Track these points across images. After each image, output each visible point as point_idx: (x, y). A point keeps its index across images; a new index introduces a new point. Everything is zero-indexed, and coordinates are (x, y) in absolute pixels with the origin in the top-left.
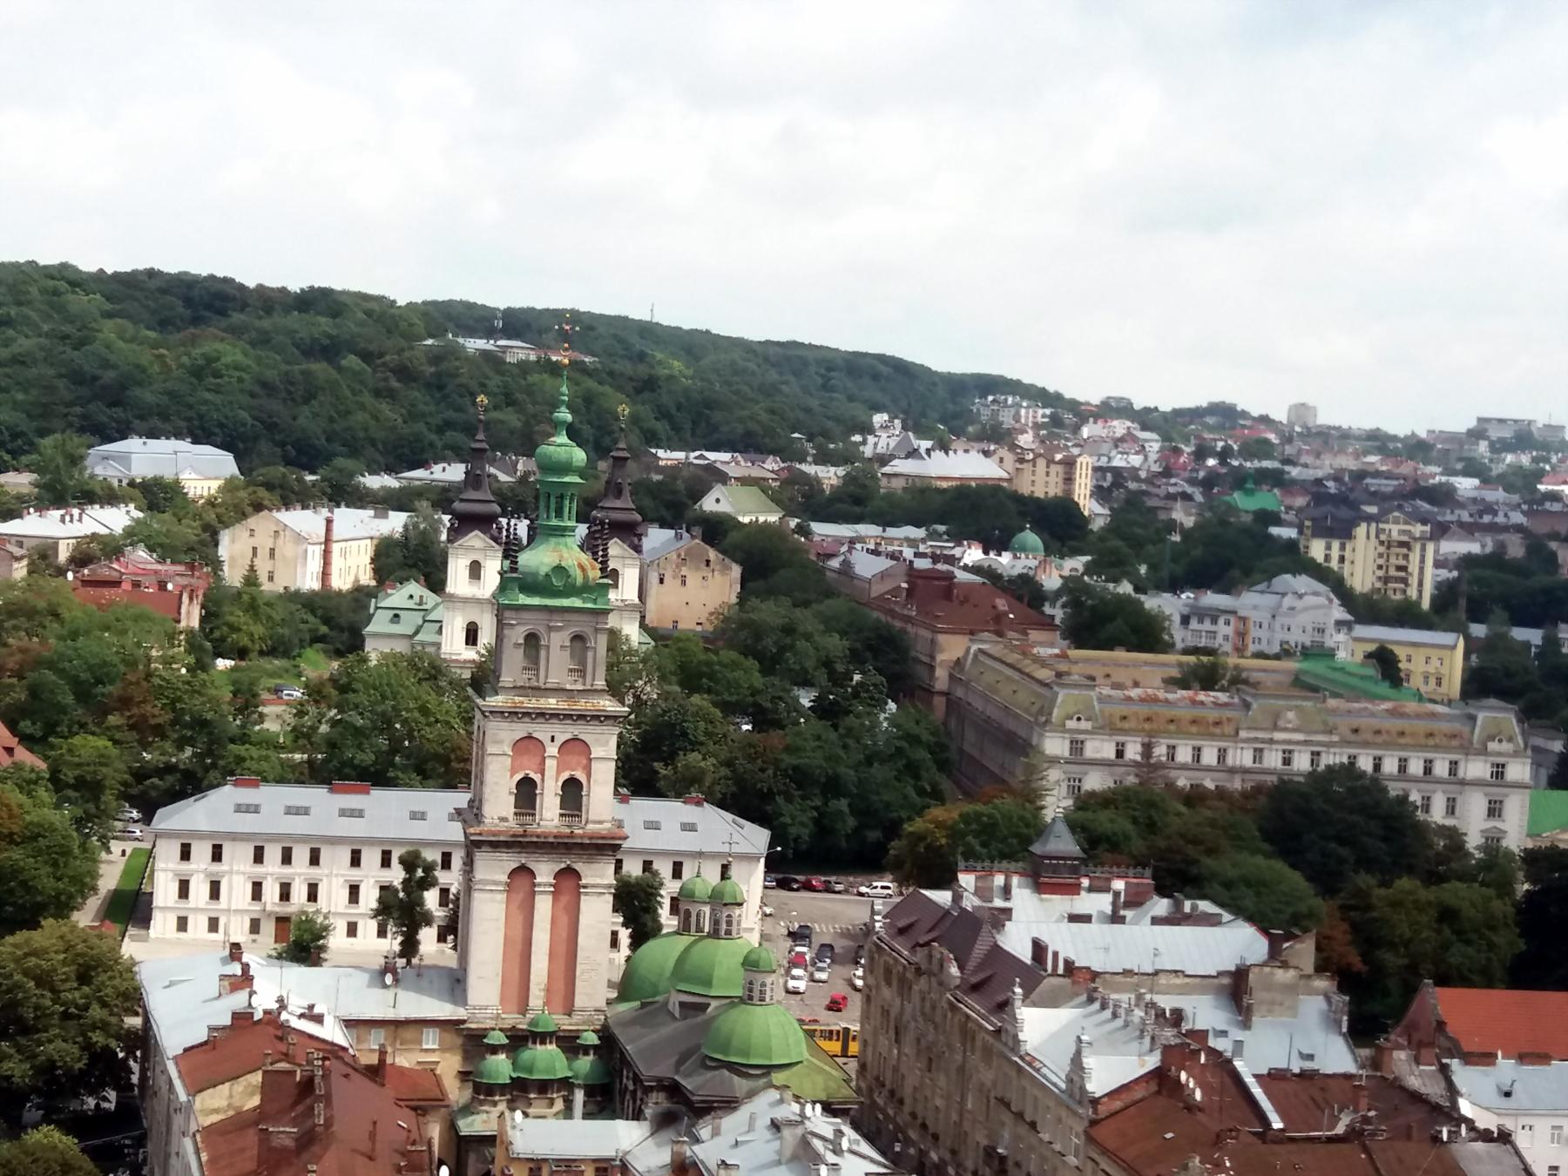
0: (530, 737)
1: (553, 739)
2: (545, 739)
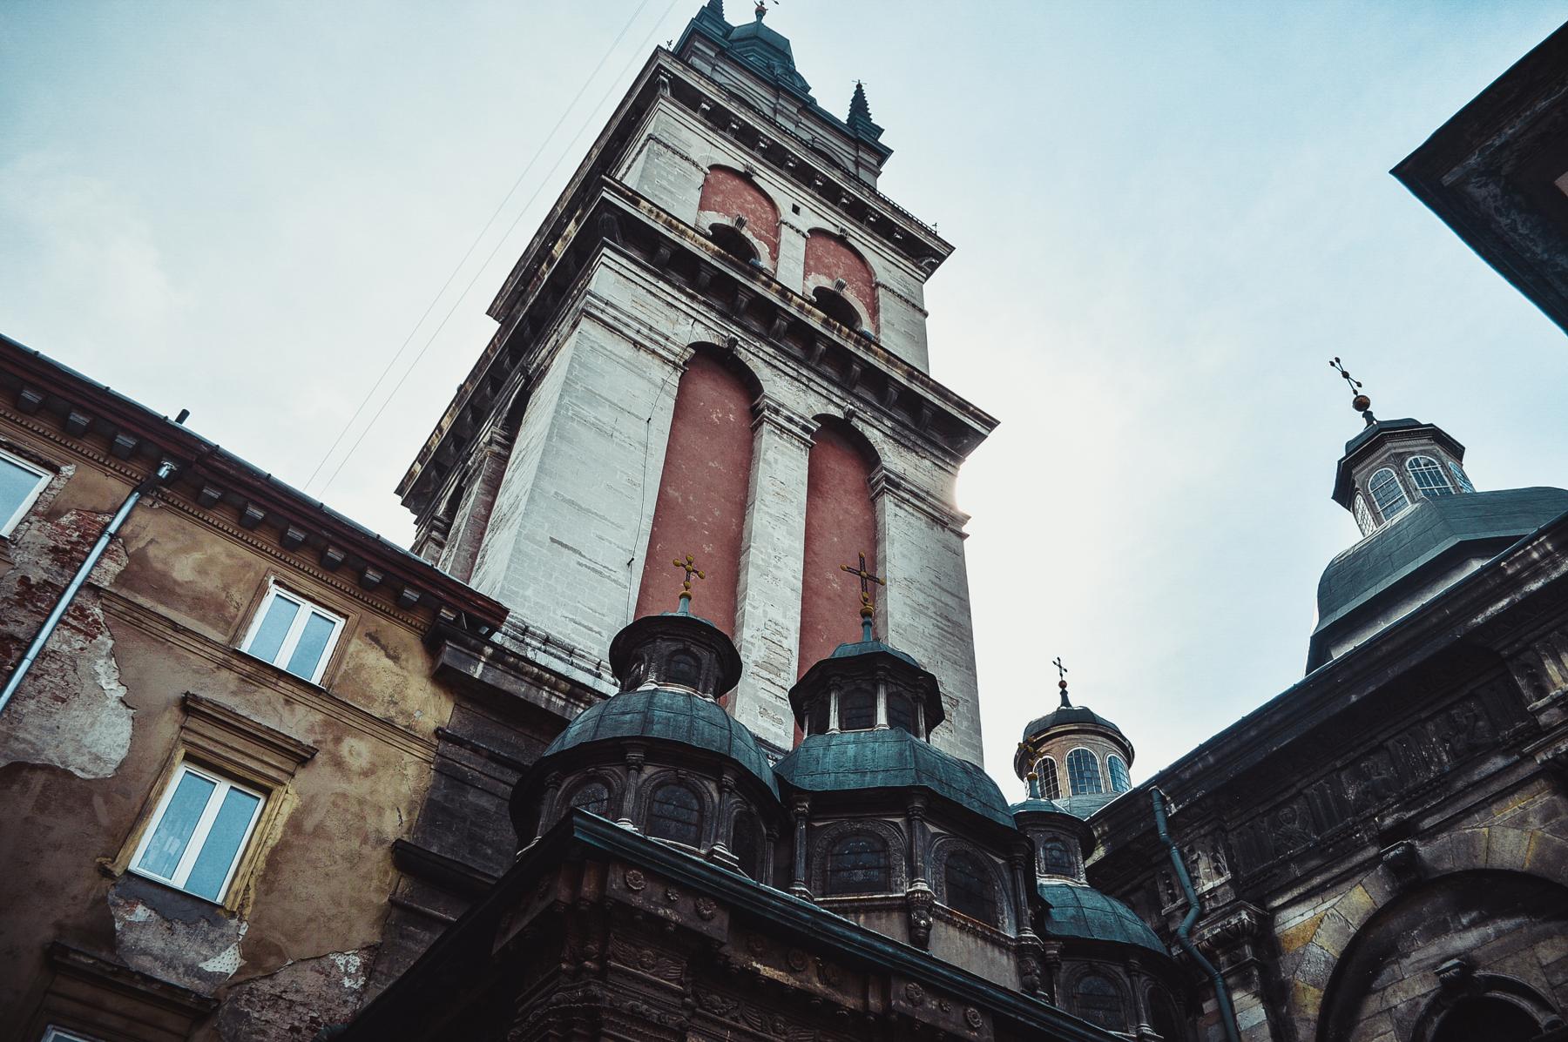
0: (746, 177)
1: (796, 210)
2: (784, 202)
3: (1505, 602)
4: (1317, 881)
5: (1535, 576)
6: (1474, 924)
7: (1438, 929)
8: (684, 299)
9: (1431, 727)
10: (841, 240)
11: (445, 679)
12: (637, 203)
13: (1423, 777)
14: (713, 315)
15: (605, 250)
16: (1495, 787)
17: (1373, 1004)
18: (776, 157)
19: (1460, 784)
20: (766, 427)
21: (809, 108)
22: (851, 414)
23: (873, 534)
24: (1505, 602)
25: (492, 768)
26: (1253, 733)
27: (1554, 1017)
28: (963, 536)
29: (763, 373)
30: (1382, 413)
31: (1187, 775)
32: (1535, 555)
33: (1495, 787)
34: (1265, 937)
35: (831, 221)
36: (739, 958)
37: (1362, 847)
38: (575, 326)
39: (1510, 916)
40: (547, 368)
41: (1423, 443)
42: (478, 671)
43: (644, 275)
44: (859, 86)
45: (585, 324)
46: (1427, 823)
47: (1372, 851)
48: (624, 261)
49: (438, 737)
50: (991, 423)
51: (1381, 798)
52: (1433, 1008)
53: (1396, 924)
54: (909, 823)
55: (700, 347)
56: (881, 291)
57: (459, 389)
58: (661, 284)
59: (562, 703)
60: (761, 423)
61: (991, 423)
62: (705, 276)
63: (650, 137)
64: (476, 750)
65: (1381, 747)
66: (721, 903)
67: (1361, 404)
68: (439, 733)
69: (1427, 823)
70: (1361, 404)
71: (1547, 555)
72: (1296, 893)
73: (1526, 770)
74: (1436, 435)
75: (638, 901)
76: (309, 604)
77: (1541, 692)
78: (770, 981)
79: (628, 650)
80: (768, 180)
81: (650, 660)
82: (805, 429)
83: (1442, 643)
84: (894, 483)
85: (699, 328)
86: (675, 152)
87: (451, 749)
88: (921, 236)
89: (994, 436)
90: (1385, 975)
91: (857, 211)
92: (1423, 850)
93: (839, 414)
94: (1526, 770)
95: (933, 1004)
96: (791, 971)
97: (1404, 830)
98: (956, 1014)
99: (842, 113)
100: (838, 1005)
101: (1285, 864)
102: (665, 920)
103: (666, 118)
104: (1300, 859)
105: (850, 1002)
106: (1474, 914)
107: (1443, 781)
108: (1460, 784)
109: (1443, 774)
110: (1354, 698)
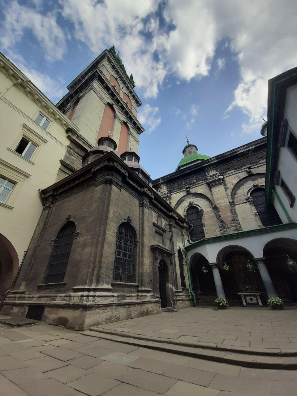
1: (123, 88)
3: (207, 164)
4: (178, 192)
5: (212, 162)
6: (194, 198)
7: (190, 198)
8: (107, 94)
9: (194, 177)
10: (128, 96)
11: (69, 137)
12: (102, 74)
13: (192, 182)
14: (111, 99)
15: (96, 80)
16: (201, 184)
17: (181, 205)
18: (121, 78)
19: (196, 183)
20: (116, 119)
21: (125, 73)
22: (127, 122)
23: (128, 139)
24: (207, 164)
25: (76, 154)
26: (174, 174)
27: (200, 208)
28: (138, 144)
29: (116, 111)
30: (190, 143)
31: (165, 178)
32: (213, 159)
33: (201, 184)
34: (170, 198)
35: (128, 93)
36: (128, 180)
37: (184, 189)
38: (90, 91)
39: (199, 198)
40: (83, 97)
41: (194, 148)
42: (74, 138)
43: (101, 87)
44: (132, 74)
45: (92, 91)
46: (191, 187)
47: (185, 189)
48: (98, 83)
49: (68, 147)
50: (144, 131)
51: (187, 184)
52: (188, 206)
53: (185, 197)
54: (139, 173)
55: (108, 103)
56: (132, 106)
57: (64, 97)
58: (104, 90)
59: (87, 147)
60: (115, 118)
61: (144, 131)
62: (110, 92)
63: (103, 65)
64: (73, 150)
65: (188, 178)
66: (128, 172)
67: (188, 142)
68: (68, 146)
69: (191, 187)
70: (188, 142)
71: (214, 160)
72: (175, 193)
73: (204, 183)
74: (196, 147)
75: (118, 167)
76: (46, 118)
77: (208, 175)
78: (131, 184)
79: (101, 141)
80: (119, 80)
81: (105, 143)
82: (121, 121)
83: (199, 167)
84: (131, 134)
85: (108, 100)
86: (107, 69)
87: (69, 149)
88: (139, 101)
89: (144, 132)
90: (183, 202)
91: (131, 92)
92: (191, 190)
93: (126, 122)
94: (204, 183)
95: (148, 191)
96: (134, 183)
97: (189, 187)
98: (151, 193)
99: (129, 77)
100: (138, 189)
101: (174, 190)
102: (121, 171)
103: (105, 62)
104: (176, 189)
105: (139, 189)
106: (194, 197)
107: (194, 183)
108: (196, 183)
109: (195, 182)
110: (187, 172)
